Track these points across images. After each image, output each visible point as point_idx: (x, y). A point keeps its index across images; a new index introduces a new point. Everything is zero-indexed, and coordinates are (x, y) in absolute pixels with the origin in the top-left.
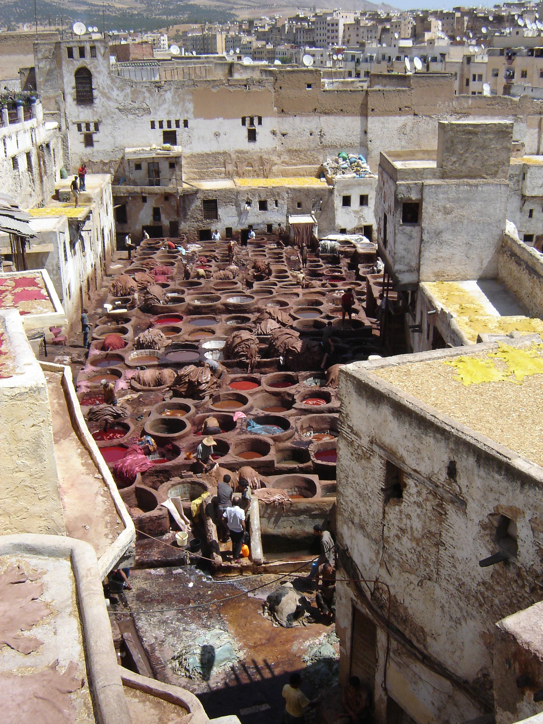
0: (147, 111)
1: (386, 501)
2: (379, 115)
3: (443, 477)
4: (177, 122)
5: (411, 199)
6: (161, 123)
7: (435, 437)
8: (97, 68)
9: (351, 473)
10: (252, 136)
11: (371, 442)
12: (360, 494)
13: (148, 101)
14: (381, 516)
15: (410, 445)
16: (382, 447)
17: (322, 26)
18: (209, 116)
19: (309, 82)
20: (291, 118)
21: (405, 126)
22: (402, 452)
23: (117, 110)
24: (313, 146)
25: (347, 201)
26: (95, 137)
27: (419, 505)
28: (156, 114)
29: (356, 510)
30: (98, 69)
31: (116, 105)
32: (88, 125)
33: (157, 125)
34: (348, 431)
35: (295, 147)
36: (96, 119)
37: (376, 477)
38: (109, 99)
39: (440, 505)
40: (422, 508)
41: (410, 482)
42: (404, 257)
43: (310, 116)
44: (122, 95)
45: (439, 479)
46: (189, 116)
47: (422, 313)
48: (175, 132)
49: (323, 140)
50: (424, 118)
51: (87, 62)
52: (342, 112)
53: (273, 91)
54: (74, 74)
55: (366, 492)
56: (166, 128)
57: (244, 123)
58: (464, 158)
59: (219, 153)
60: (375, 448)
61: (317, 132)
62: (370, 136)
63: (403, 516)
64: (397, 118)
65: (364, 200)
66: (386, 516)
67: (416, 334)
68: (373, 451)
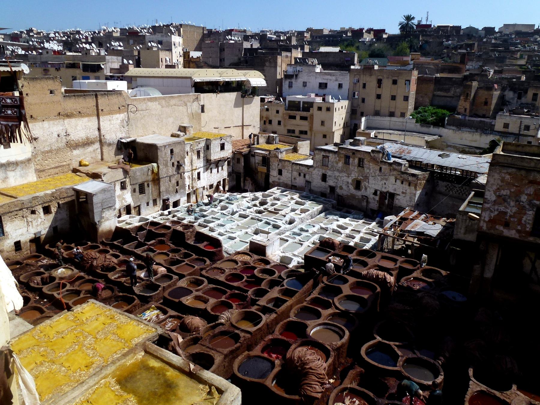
2: (107, 115)
19: (52, 89)
20: (41, 123)
43: (56, 119)
52: (80, 114)
61: (63, 134)
62: (103, 132)
64: (118, 115)
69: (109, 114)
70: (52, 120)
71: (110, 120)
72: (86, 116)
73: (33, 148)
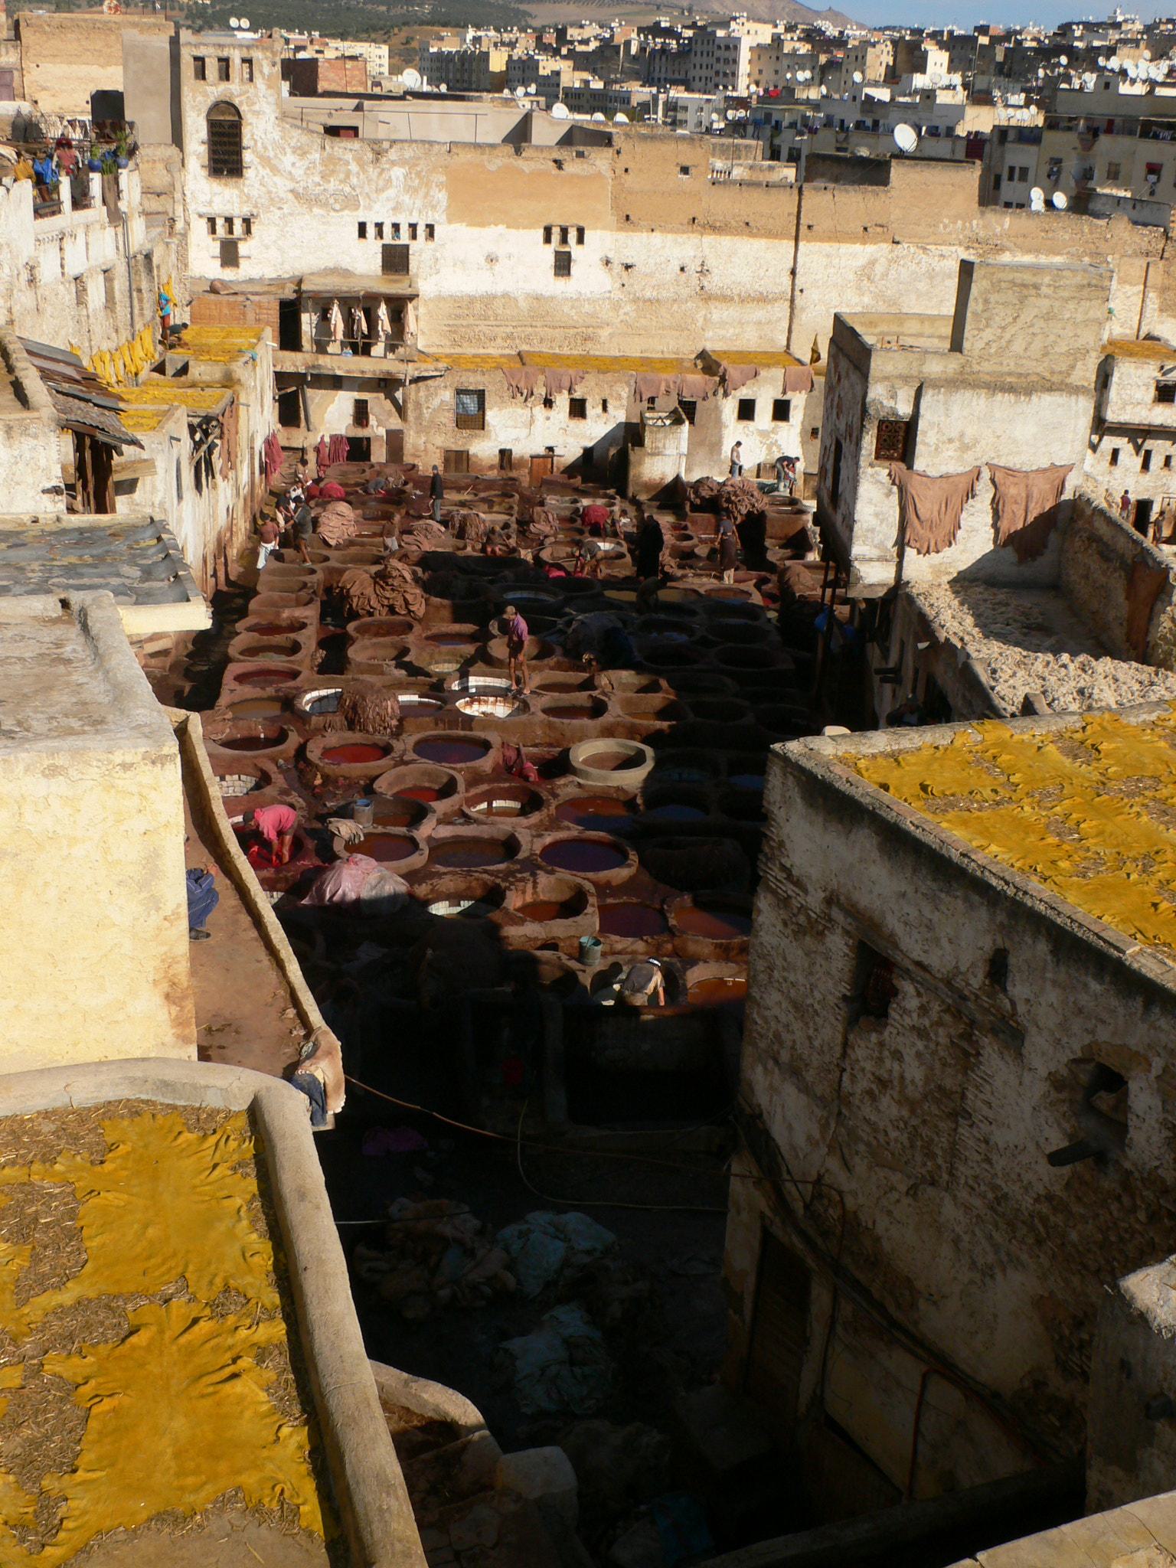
0: (351, 202)
1: (851, 1023)
2: (822, 240)
3: (977, 980)
4: (413, 227)
5: (895, 414)
6: (379, 226)
7: (966, 899)
8: (254, 104)
9: (779, 962)
10: (563, 265)
11: (831, 900)
12: (796, 1006)
13: (354, 180)
14: (838, 1050)
15: (914, 913)
16: (853, 911)
17: (705, 48)
18: (478, 220)
19: (686, 163)
21: (872, 263)
22: (893, 923)
23: (290, 196)
24: (685, 292)
25: (746, 410)
26: (243, 248)
27: (921, 1033)
28: (369, 208)
29: (785, 1036)
30: (256, 107)
31: (290, 185)
32: (229, 221)
33: (371, 231)
34: (781, 876)
35: (648, 294)
36: (246, 211)
37: (834, 971)
38: (275, 170)
39: (967, 1036)
40: (929, 1039)
41: (907, 987)
42: (873, 530)
43: (684, 232)
44: (302, 164)
45: (968, 984)
46: (436, 216)
47: (903, 644)
48: (407, 247)
49: (706, 284)
50: (912, 250)
51: (234, 89)
52: (747, 228)
53: (609, 174)
54: (204, 115)
55: (809, 1001)
56: (388, 239)
57: (548, 239)
58: (1007, 336)
59: (495, 297)
60: (836, 914)
61: (693, 267)
62: (800, 281)
63: (887, 1053)
64: (858, 247)
65: (781, 411)
66: (849, 1051)
67: (888, 688)
68: (830, 920)
69: (829, 239)
70: (671, 231)
71: (828, 256)
72: (762, 236)
73: (618, 285)
